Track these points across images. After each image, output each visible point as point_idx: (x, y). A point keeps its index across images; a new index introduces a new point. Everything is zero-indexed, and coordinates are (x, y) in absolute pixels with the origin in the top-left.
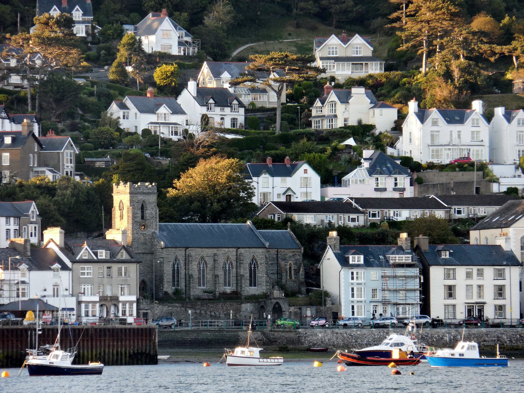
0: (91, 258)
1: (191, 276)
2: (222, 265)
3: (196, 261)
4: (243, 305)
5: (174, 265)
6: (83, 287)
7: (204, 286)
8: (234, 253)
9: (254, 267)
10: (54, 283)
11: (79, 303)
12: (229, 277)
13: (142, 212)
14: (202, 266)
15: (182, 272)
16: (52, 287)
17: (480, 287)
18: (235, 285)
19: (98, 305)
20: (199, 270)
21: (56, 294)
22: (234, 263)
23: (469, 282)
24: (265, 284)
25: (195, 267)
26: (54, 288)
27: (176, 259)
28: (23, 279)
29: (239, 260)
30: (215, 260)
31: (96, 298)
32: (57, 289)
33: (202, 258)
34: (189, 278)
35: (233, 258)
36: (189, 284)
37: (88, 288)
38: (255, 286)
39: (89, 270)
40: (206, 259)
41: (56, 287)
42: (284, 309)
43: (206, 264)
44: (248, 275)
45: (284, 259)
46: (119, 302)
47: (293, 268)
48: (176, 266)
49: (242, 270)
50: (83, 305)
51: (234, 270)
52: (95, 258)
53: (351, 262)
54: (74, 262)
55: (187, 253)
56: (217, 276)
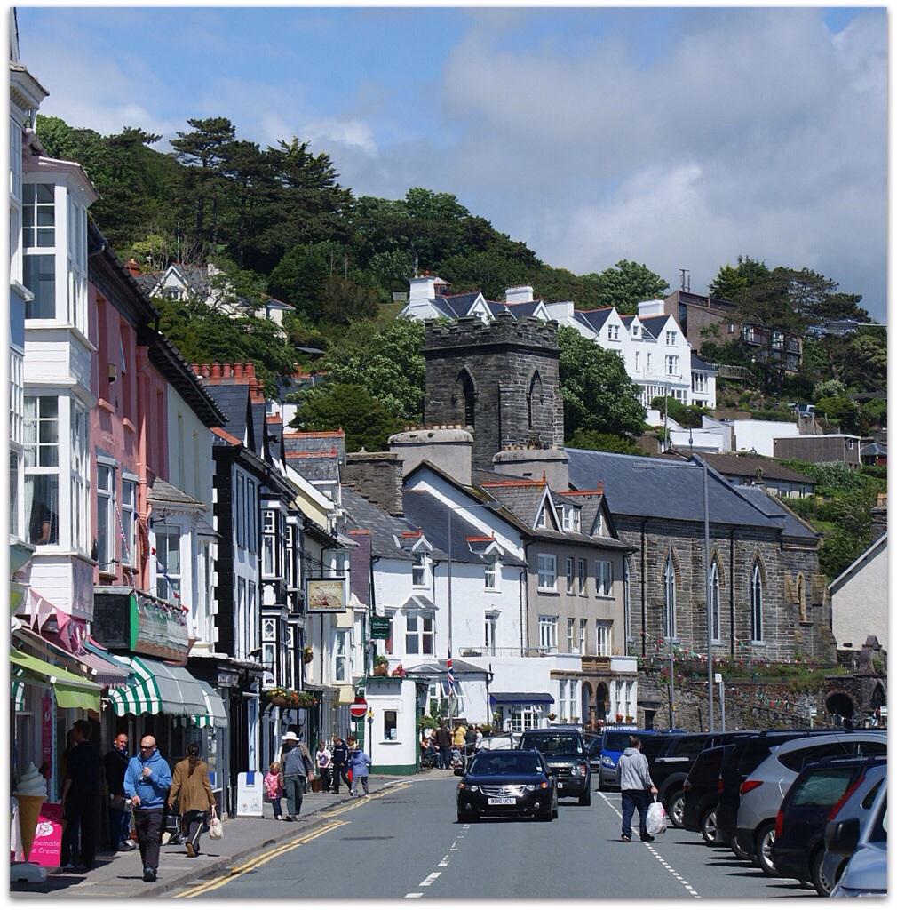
9: (758, 584)
19: (580, 683)
22: (727, 573)
24: (777, 632)
38: (759, 639)
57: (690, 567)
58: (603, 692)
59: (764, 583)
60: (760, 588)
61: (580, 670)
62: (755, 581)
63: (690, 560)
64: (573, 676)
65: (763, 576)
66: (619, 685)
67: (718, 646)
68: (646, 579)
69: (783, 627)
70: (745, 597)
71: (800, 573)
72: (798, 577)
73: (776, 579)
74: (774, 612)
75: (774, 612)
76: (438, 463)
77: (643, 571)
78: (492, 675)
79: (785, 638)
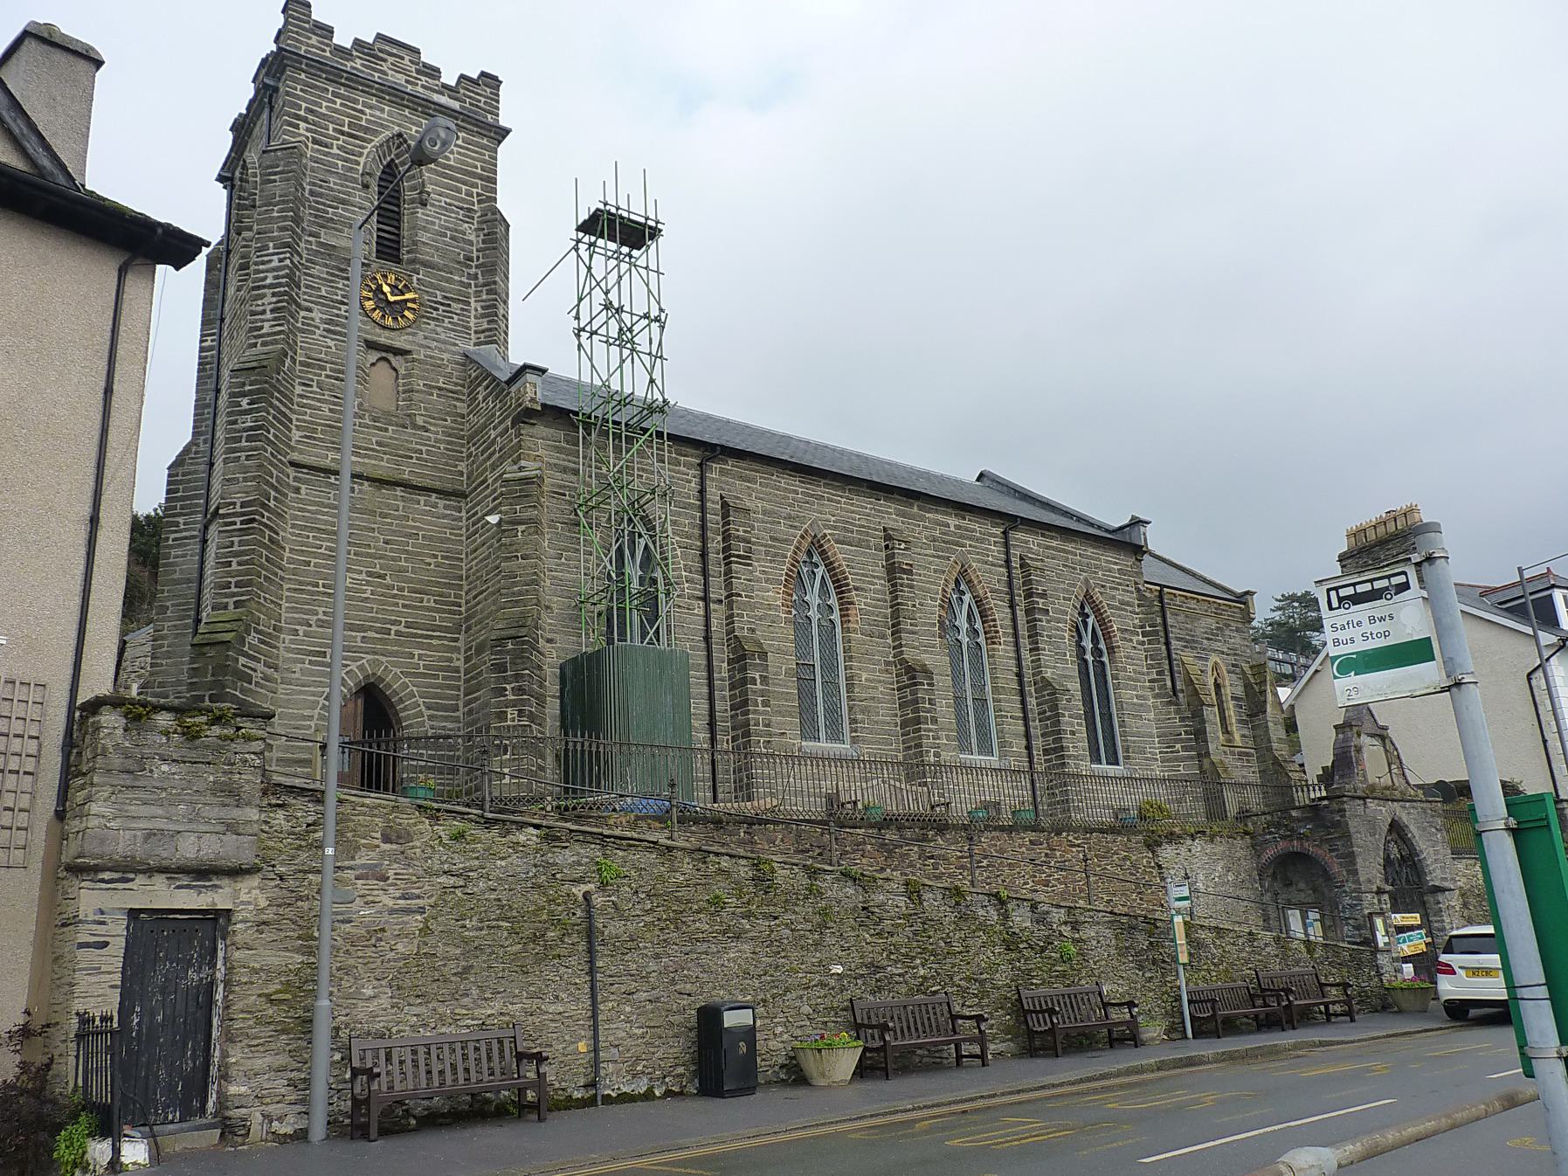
2: (933, 608)
3: (775, 557)
4: (1167, 852)
7: (835, 736)
8: (996, 552)
9: (1097, 652)
12: (981, 702)
14: (813, 598)
18: (1018, 745)
20: (802, 627)
22: (1001, 614)
24: (1155, 747)
29: (1023, 589)
30: (892, 570)
33: (817, 547)
34: (740, 657)
35: (990, 578)
36: (741, 705)
40: (840, 554)
42: (1435, 877)
43: (841, 587)
44: (1075, 686)
45: (1190, 643)
47: (1227, 691)
48: (633, 571)
49: (1046, 655)
51: (1004, 649)
55: (713, 493)
56: (911, 675)
57: (881, 584)
59: (1111, 650)
60: (1105, 659)
62: (1087, 644)
63: (880, 571)
65: (1108, 636)
68: (717, 592)
69: (1168, 739)
70: (1060, 667)
71: (1214, 658)
72: (1210, 664)
73: (1143, 643)
77: (705, 572)
79: (1176, 759)
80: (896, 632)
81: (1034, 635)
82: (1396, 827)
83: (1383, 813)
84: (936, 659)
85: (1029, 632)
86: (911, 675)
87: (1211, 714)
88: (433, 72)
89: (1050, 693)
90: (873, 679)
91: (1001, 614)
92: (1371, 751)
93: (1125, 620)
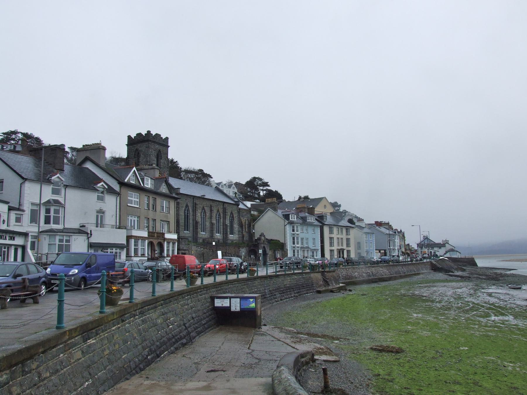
0: (138, 184)
1: (197, 223)
5: (185, 211)
6: (130, 218)
10: (98, 209)
11: (129, 238)
13: (157, 161)
15: (191, 217)
16: (96, 214)
17: (342, 239)
21: (100, 223)
22: (222, 215)
23: (338, 236)
24: (237, 233)
25: (199, 215)
26: (97, 216)
27: (187, 206)
28: (55, 197)
31: (145, 234)
32: (102, 217)
35: (221, 211)
37: (134, 221)
39: (134, 199)
41: (100, 215)
45: (242, 216)
46: (165, 239)
50: (132, 241)
51: (222, 220)
52: (142, 185)
53: (290, 219)
54: (122, 184)
58: (161, 246)
61: (147, 236)
64: (143, 239)
66: (168, 243)
67: (218, 236)
69: (239, 232)
70: (228, 222)
74: (236, 226)
75: (236, 226)
76: (92, 157)
78: (91, 235)
80: (211, 218)
81: (225, 218)
82: (264, 247)
83: (263, 245)
84: (214, 221)
85: (225, 218)
86: (212, 224)
87: (244, 227)
88: (162, 138)
89: (226, 225)
90: (208, 224)
91: (222, 215)
92: (263, 238)
93: (235, 215)
